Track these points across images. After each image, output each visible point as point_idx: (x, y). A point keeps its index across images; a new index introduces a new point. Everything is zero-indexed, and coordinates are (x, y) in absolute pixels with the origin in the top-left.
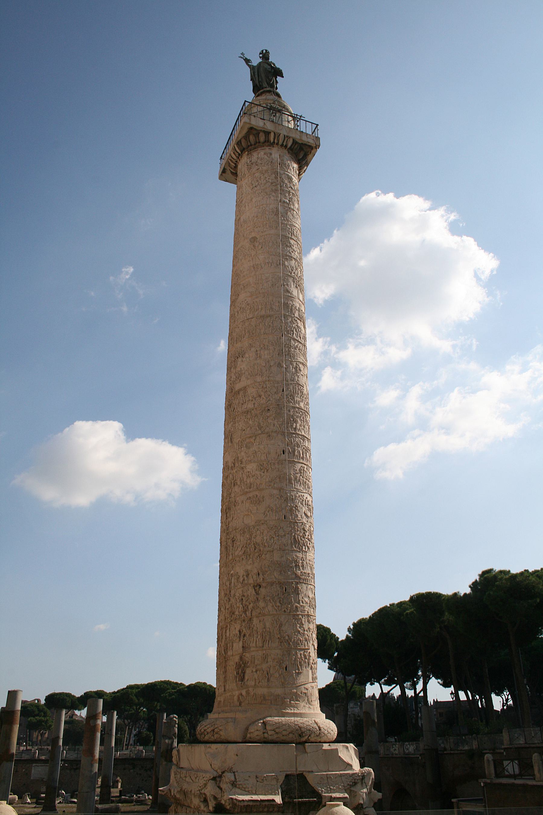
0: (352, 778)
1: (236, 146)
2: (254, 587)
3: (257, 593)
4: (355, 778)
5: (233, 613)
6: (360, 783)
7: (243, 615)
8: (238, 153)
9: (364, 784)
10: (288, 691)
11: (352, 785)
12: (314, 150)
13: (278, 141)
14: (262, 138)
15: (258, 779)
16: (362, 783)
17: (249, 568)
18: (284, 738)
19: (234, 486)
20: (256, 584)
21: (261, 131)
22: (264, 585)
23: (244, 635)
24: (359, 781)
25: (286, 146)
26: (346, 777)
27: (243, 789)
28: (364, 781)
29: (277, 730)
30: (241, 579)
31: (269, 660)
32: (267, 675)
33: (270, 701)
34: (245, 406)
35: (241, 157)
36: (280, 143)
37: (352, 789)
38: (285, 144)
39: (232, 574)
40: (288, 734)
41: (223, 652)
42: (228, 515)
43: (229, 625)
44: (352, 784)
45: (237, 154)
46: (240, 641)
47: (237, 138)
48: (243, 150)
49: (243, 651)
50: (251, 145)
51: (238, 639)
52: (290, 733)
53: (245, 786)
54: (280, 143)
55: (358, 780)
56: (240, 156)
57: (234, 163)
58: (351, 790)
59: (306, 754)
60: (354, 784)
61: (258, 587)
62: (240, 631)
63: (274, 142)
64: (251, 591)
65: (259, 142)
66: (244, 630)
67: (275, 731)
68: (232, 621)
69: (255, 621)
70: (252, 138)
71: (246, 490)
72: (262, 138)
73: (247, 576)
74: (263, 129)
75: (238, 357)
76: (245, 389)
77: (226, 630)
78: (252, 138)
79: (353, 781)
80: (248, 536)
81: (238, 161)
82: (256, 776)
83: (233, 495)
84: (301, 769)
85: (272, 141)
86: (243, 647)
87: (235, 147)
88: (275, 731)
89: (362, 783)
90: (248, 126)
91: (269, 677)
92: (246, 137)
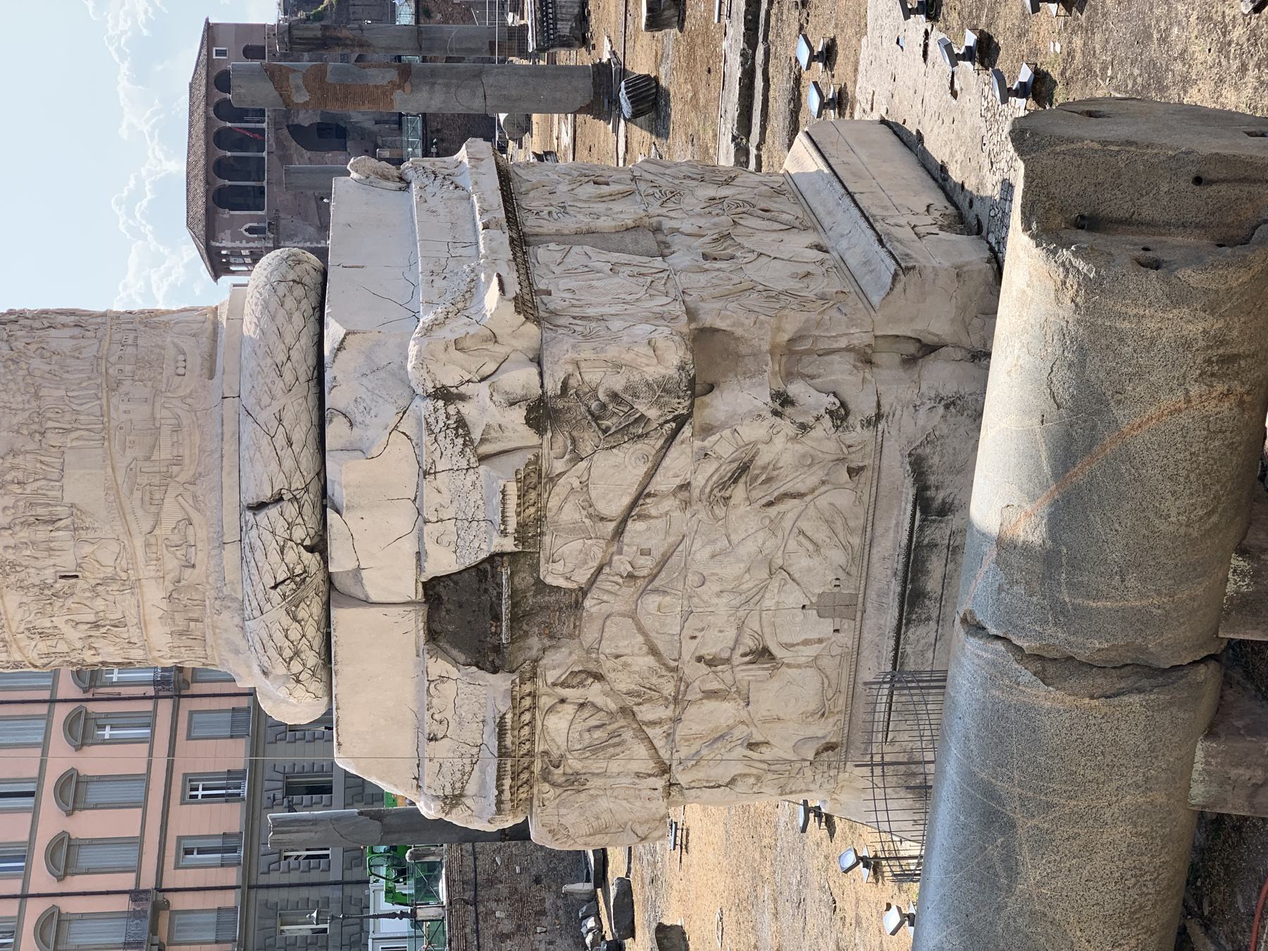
0: (443, 434)
4: (441, 424)
6: (460, 405)
9: (463, 389)
10: (152, 568)
11: (464, 436)
15: (440, 736)
16: (462, 398)
18: (311, 631)
24: (452, 409)
26: (438, 453)
27: (466, 777)
28: (454, 390)
29: (288, 653)
31: (49, 625)
32: (104, 630)
33: (192, 624)
37: (476, 435)
40: (299, 622)
44: (460, 441)
52: (295, 619)
53: (458, 775)
55: (448, 418)
58: (482, 441)
59: (364, 573)
60: (460, 431)
67: (291, 659)
79: (451, 433)
82: (430, 740)
84: (409, 589)
88: (291, 659)
89: (462, 398)
91: (108, 622)
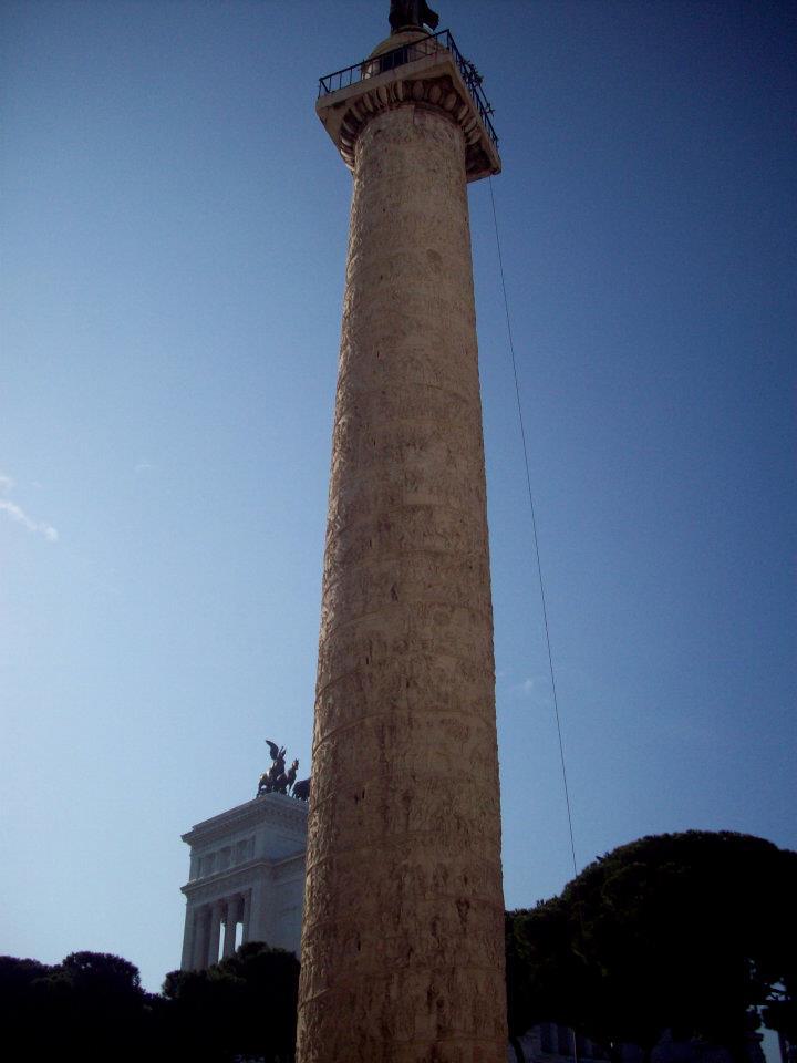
1: (400, 86)
2: (459, 903)
3: (464, 920)
5: (411, 950)
7: (439, 959)
8: (396, 95)
12: (488, 172)
13: (467, 124)
14: (451, 103)
17: (447, 862)
19: (408, 685)
20: (462, 900)
21: (456, 91)
22: (473, 904)
23: (440, 1005)
25: (468, 140)
30: (430, 881)
34: (428, 542)
35: (398, 107)
36: (467, 129)
38: (470, 135)
39: (406, 866)
41: (377, 1033)
42: (387, 740)
43: (396, 977)
45: (393, 98)
46: (430, 1013)
47: (416, 74)
48: (409, 98)
49: (438, 1036)
50: (428, 101)
51: (427, 1009)
54: (467, 129)
56: (396, 103)
57: (373, 105)
61: (464, 908)
62: (430, 994)
63: (461, 121)
64: (451, 913)
65: (442, 106)
66: (442, 991)
68: (408, 966)
69: (461, 976)
70: (436, 92)
71: (436, 703)
72: (451, 103)
73: (445, 877)
74: (460, 92)
75: (408, 445)
76: (429, 509)
77: (388, 985)
78: (436, 92)
80: (445, 798)
81: (387, 108)
83: (402, 704)
85: (460, 117)
86: (439, 1027)
87: (396, 85)
90: (446, 70)
92: (428, 83)
